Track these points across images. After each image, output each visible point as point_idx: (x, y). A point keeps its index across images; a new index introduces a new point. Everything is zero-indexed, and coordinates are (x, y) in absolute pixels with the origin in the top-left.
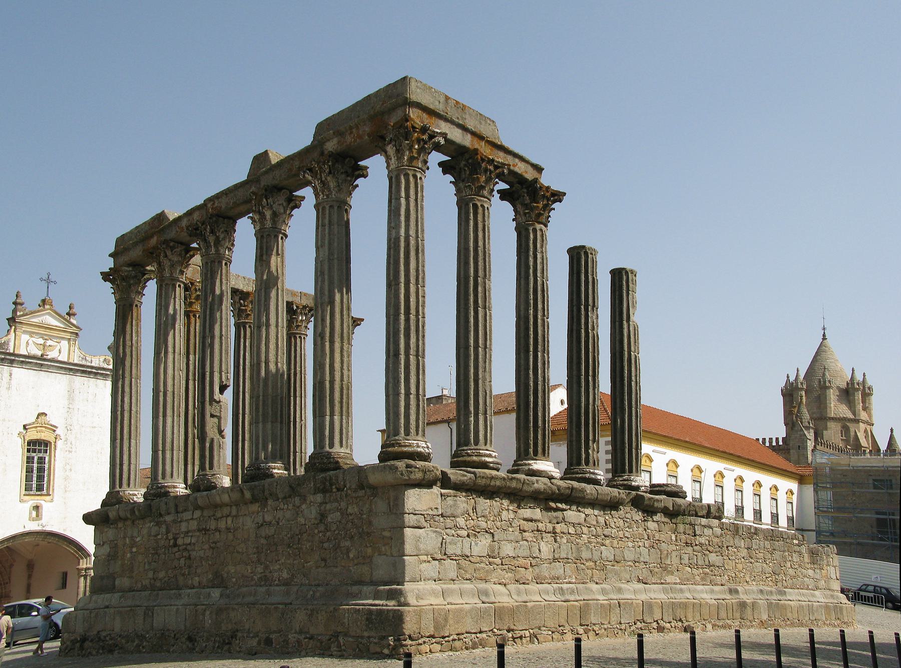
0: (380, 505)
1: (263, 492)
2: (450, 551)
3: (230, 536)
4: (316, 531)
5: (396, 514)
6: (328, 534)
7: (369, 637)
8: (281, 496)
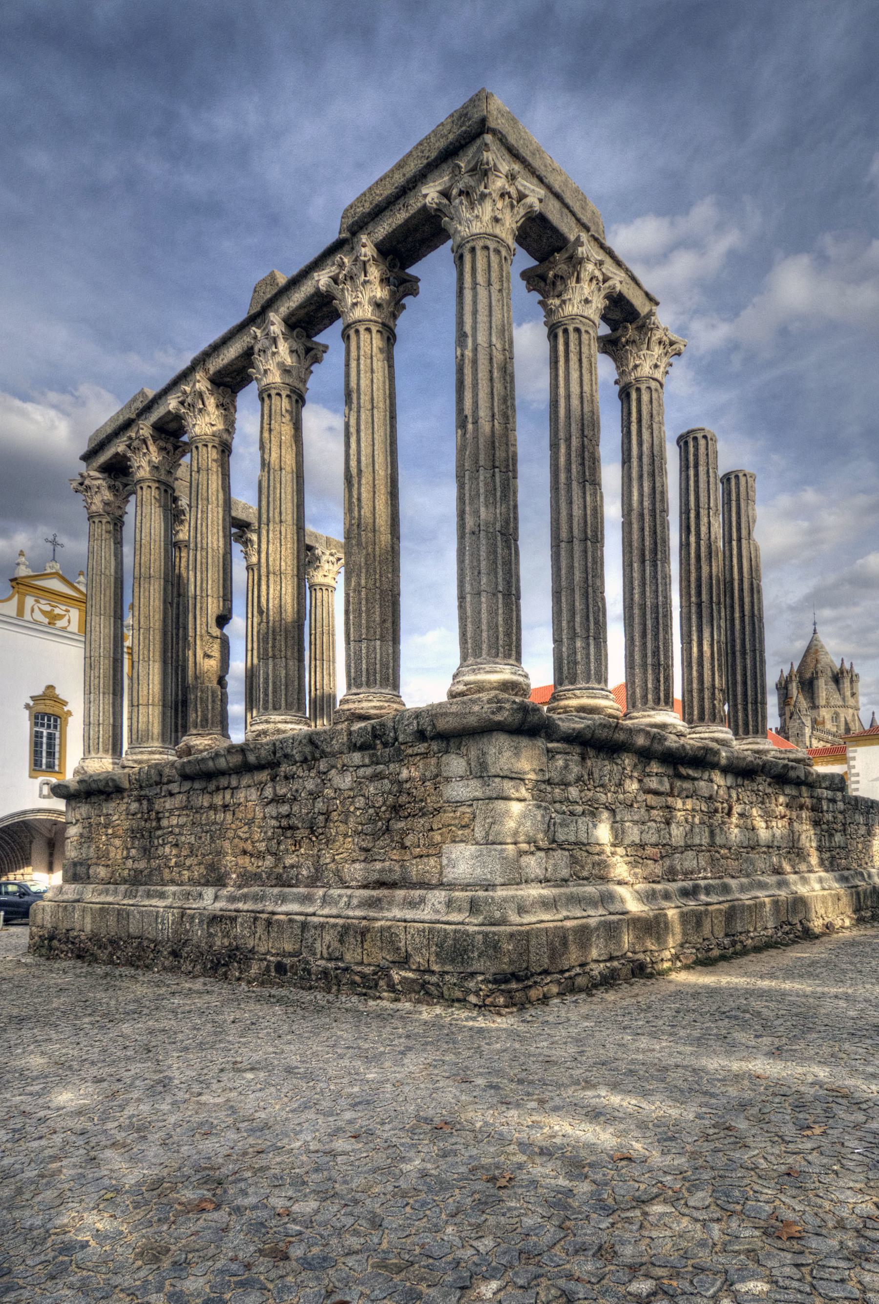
0: (456, 764)
1: (274, 753)
2: (561, 837)
3: (229, 817)
4: (352, 809)
5: (481, 777)
6: (371, 811)
7: (443, 974)
8: (298, 757)
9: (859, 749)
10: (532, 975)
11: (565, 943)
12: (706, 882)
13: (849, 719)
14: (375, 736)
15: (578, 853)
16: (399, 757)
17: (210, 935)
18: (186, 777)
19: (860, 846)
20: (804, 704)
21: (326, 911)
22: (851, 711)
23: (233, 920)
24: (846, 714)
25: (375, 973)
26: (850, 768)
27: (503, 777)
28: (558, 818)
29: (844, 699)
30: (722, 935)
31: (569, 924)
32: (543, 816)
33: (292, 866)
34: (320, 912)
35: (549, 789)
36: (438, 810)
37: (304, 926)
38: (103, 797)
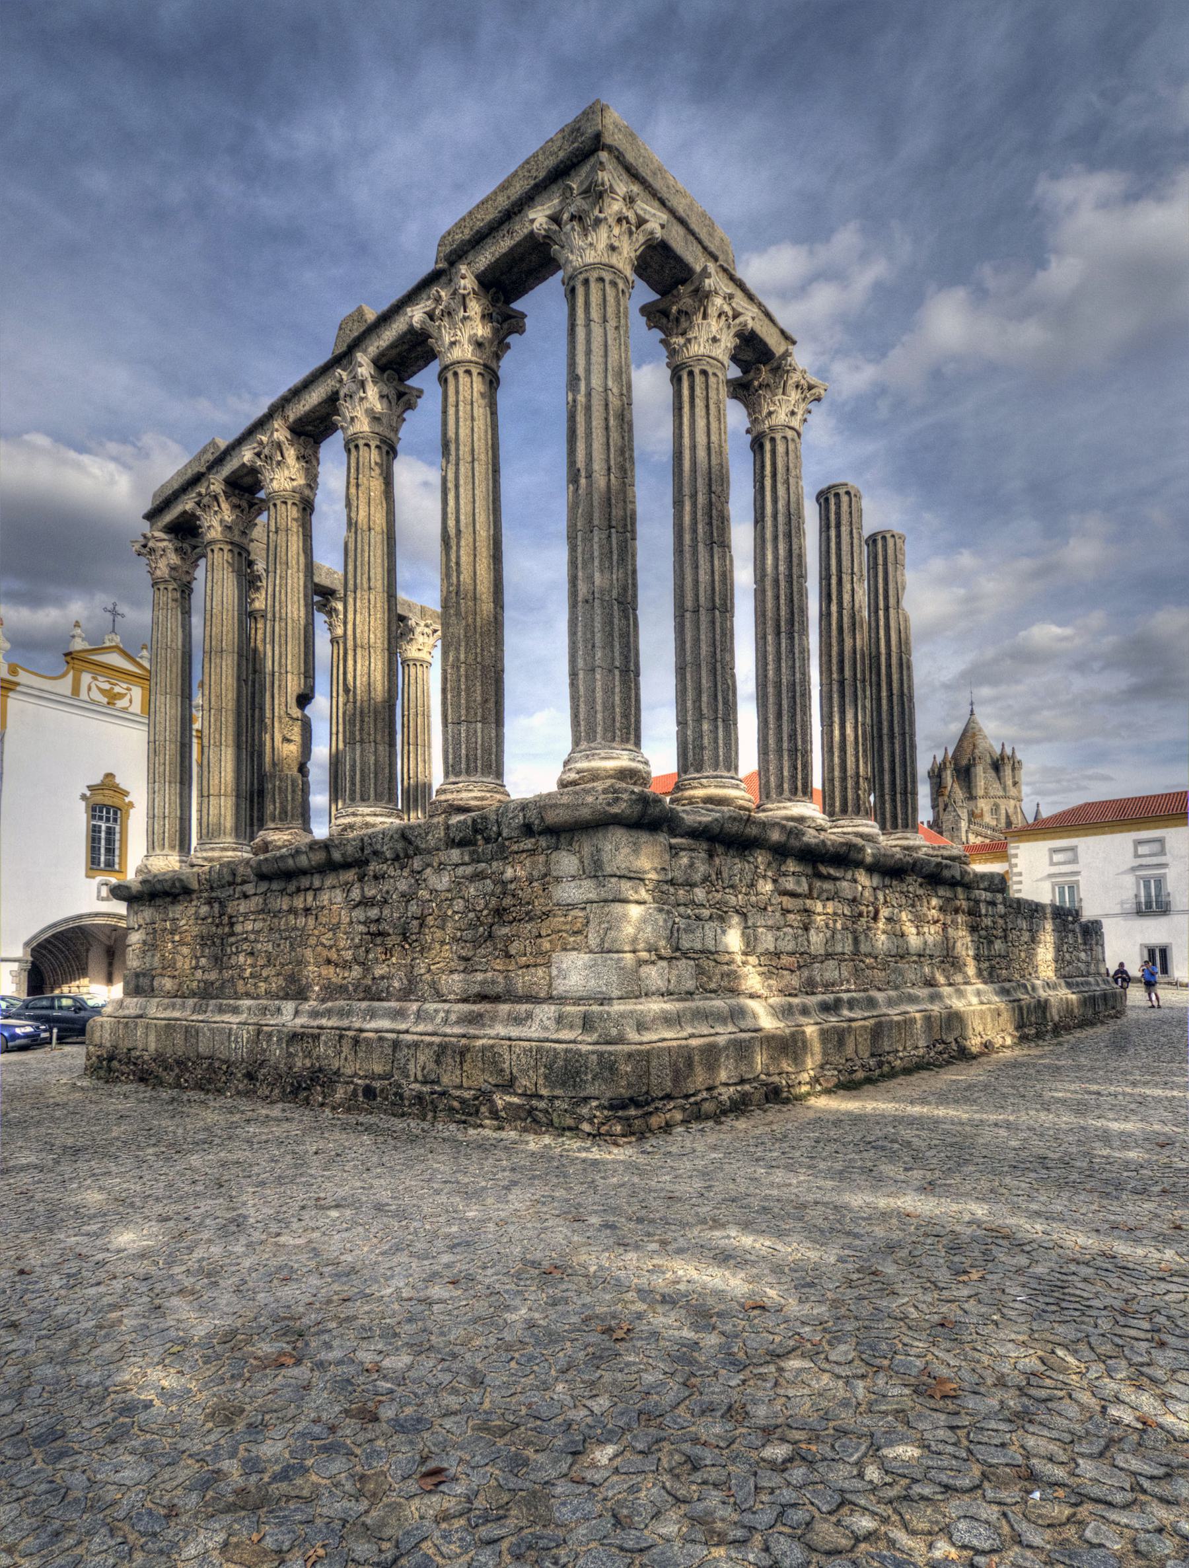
0: (567, 862)
1: (362, 849)
2: (685, 944)
3: (311, 921)
4: (450, 913)
6: (471, 915)
7: (552, 1099)
8: (389, 855)
9: (1022, 845)
10: (653, 1100)
11: (690, 1064)
12: (849, 995)
13: (1011, 811)
14: (476, 831)
15: (707, 964)
16: (503, 854)
17: (290, 1055)
18: (262, 877)
19: (1023, 954)
20: (959, 794)
21: (421, 1028)
22: (1012, 802)
23: (316, 1037)
24: (1007, 806)
25: (476, 1098)
26: (1011, 866)
27: (620, 877)
28: (682, 923)
29: (1004, 789)
30: (867, 1054)
31: (694, 1042)
32: (665, 921)
33: (382, 978)
34: (413, 1029)
35: (672, 890)
36: (547, 914)
37: (396, 1045)
38: (168, 899)
